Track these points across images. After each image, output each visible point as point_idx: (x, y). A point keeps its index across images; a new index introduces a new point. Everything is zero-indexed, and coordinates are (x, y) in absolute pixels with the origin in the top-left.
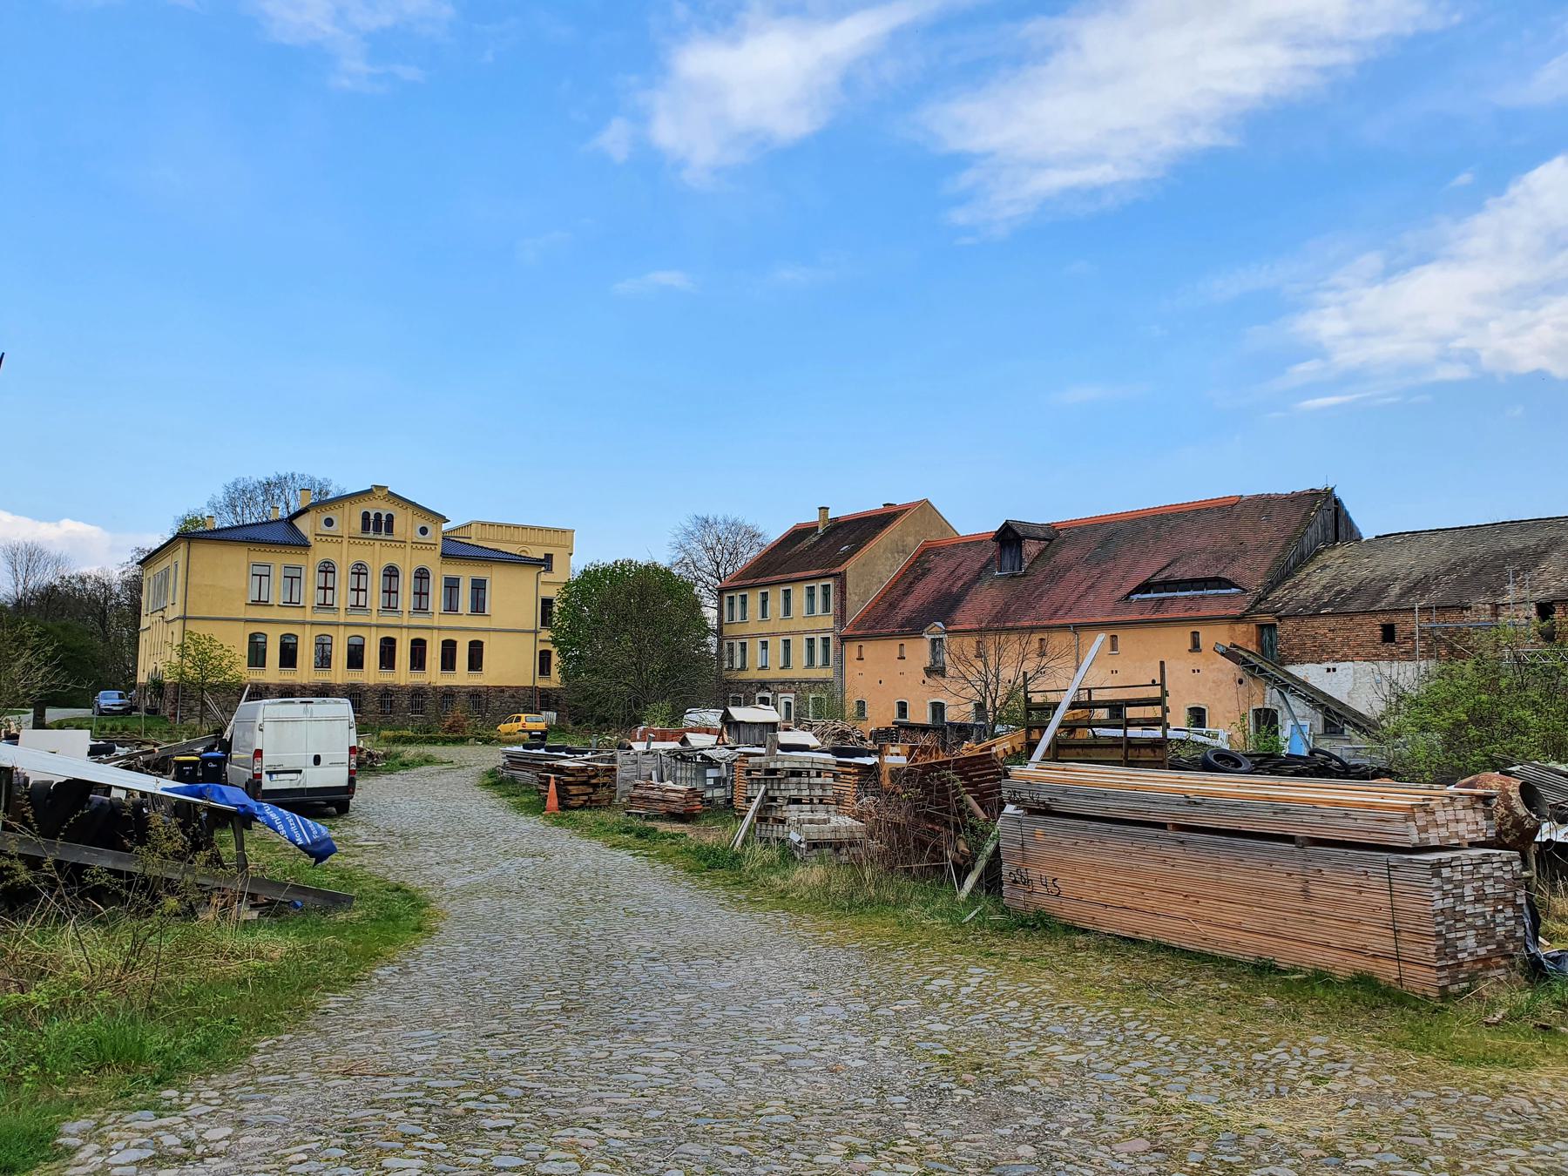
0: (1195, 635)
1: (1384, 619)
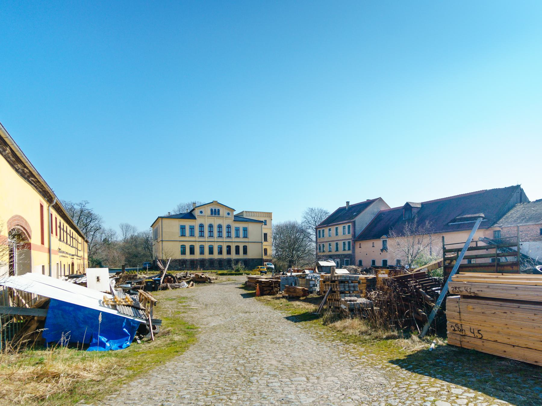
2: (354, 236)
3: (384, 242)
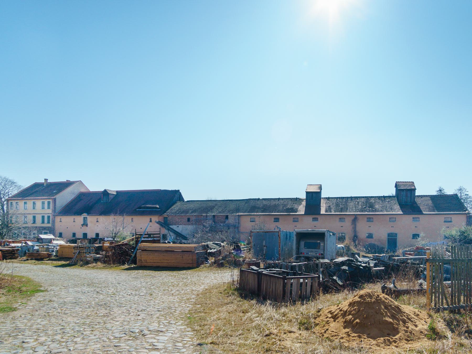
0: (151, 219)
1: (188, 217)
2: (54, 210)
3: (85, 219)
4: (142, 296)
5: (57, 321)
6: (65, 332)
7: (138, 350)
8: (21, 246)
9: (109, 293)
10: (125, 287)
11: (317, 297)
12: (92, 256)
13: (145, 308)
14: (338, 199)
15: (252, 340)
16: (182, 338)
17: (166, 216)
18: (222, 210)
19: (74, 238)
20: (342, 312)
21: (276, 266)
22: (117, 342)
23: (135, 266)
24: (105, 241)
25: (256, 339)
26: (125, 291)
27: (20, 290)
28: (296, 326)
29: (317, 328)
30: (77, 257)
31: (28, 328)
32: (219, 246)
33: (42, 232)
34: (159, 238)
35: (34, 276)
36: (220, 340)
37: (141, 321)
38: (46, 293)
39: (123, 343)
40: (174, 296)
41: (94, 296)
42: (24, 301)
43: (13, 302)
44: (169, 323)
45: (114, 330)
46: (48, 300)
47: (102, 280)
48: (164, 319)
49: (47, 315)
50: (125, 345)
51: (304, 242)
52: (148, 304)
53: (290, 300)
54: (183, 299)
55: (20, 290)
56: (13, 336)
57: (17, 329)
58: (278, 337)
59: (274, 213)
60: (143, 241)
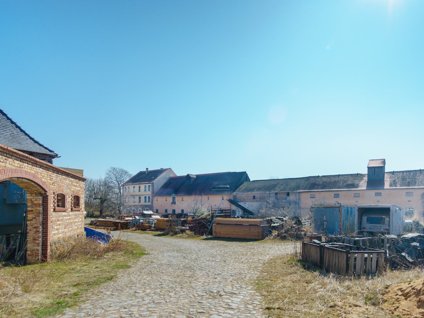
0: (223, 197)
1: (253, 195)
2: (153, 192)
3: (174, 199)
4: (218, 262)
5: (157, 278)
6: (163, 287)
7: (216, 308)
8: (132, 220)
9: (193, 258)
10: (204, 254)
11: (384, 273)
12: (179, 228)
13: (220, 273)
14: (405, 173)
15: (316, 309)
16: (252, 301)
17: (236, 195)
18: (284, 188)
19: (166, 214)
20: (415, 291)
21: (338, 240)
22: (200, 299)
23: (211, 236)
24: (188, 216)
25: (320, 309)
26: (205, 257)
27: (132, 253)
28: (361, 300)
29: (385, 305)
30: (169, 228)
31: (138, 282)
32: (281, 220)
33: (145, 209)
34: (230, 214)
35: (140, 242)
36: (286, 306)
37: (218, 283)
38: (149, 256)
39: (205, 301)
40: (243, 264)
41: (182, 260)
42: (135, 261)
43: (128, 261)
44: (241, 287)
45: (197, 289)
46: (150, 261)
47: (187, 247)
48: (236, 283)
49: (150, 273)
50: (206, 302)
51: (366, 217)
52: (223, 269)
53: (354, 273)
54: (252, 266)
55: (132, 253)
56: (129, 287)
57: (131, 281)
58: (343, 310)
59: (411, 186)
60: (217, 216)
